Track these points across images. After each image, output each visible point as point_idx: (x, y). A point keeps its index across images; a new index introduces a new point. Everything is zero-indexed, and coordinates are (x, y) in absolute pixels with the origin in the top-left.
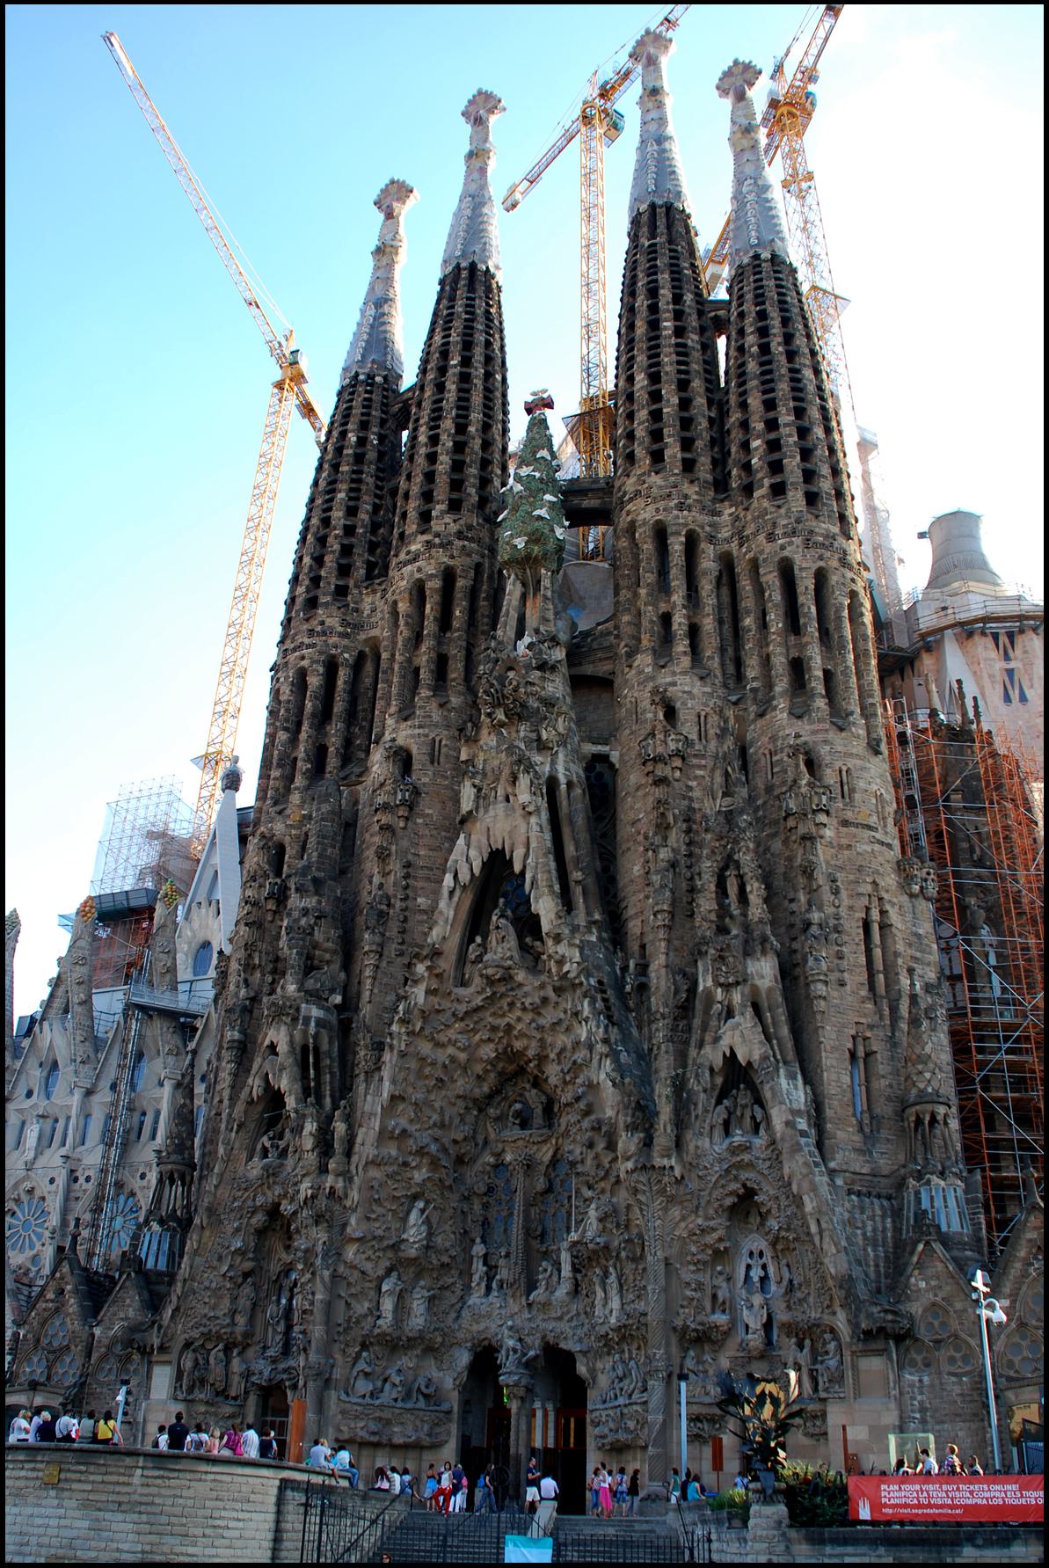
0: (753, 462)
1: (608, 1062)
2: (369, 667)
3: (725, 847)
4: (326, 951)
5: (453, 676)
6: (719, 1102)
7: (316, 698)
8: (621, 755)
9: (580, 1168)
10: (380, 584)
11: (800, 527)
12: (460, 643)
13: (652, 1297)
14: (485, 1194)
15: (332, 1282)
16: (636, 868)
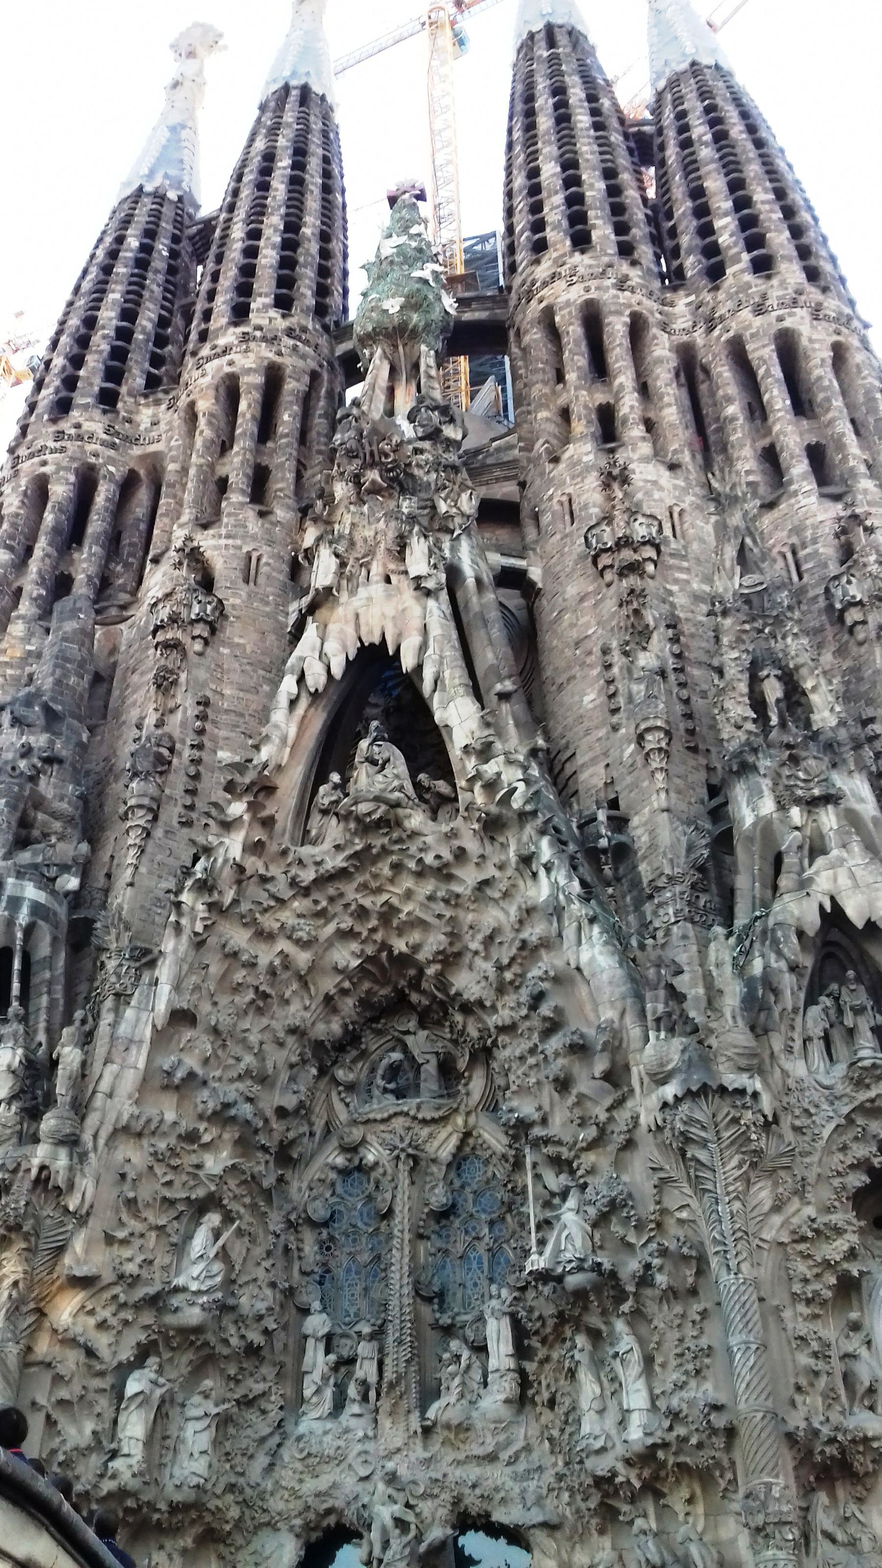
0: (720, 241)
1: (596, 929)
2: (143, 495)
3: (760, 631)
4: (55, 815)
5: (280, 486)
6: (811, 1000)
7: (60, 510)
8: (547, 572)
9: (537, 1131)
10: (166, 392)
11: (803, 298)
12: (288, 450)
13: (744, 1362)
14: (326, 1224)
15: (21, 1372)
16: (587, 699)
